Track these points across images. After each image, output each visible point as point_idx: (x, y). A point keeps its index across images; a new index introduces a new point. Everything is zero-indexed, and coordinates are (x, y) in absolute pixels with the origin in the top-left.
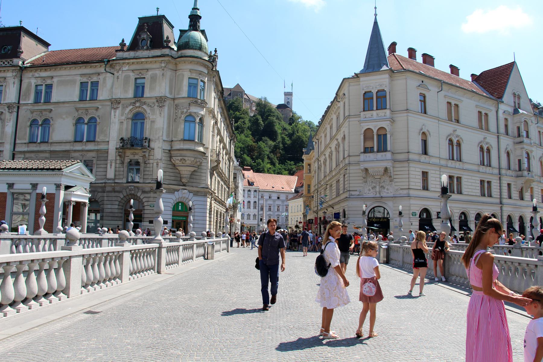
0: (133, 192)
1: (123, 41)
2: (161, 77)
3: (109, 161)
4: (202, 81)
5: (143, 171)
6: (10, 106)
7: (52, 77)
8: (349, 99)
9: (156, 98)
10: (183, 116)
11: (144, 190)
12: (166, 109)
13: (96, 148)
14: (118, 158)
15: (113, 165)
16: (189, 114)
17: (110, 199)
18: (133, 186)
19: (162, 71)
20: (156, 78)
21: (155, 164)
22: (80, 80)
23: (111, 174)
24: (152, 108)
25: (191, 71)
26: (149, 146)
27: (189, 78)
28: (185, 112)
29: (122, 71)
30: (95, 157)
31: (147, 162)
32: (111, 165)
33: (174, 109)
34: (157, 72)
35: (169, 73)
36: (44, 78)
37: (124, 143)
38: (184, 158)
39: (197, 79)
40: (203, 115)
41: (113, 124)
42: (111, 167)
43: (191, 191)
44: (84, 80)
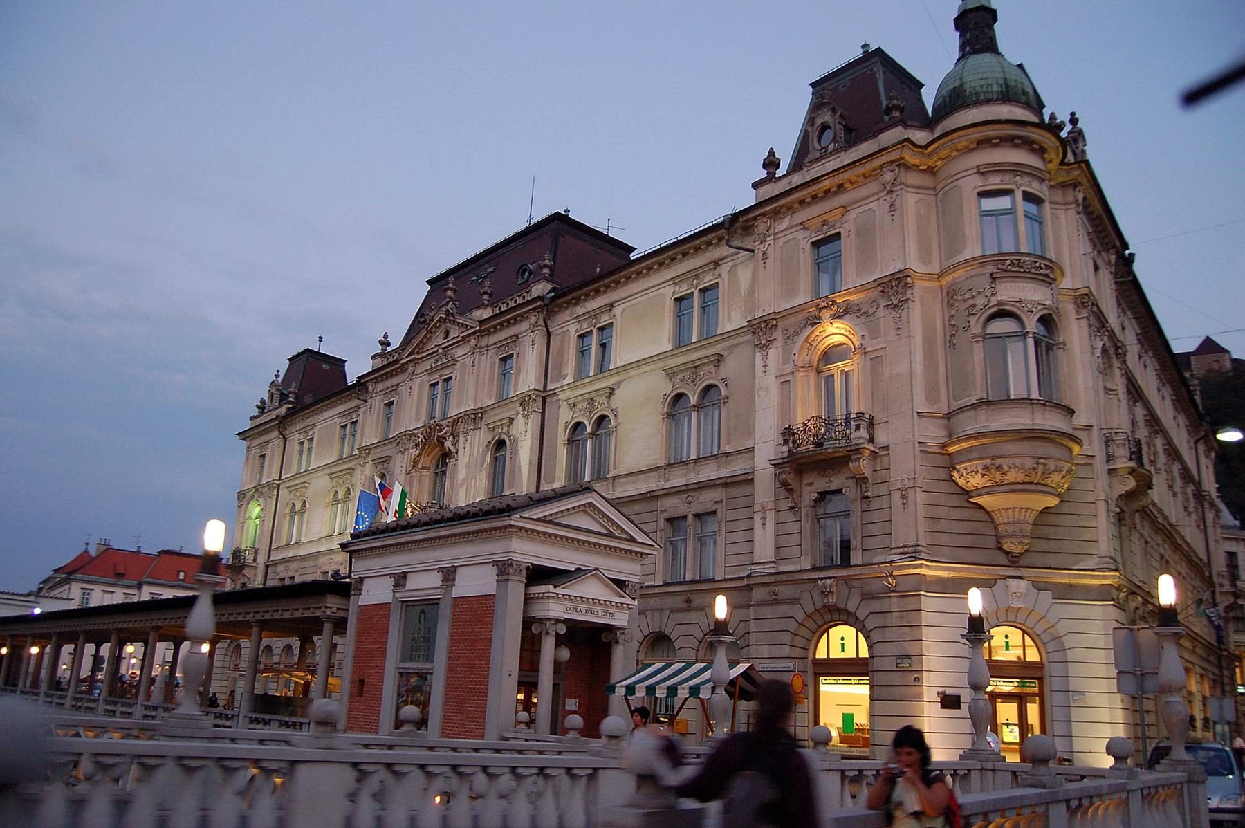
0: (831, 600)
1: (771, 153)
2: (887, 216)
3: (757, 508)
5: (859, 527)
6: (524, 402)
7: (611, 306)
9: (878, 283)
10: (973, 319)
11: (867, 588)
12: (914, 312)
13: (723, 473)
14: (782, 493)
15: (770, 516)
17: (766, 625)
18: (830, 578)
19: (888, 197)
20: (873, 224)
21: (896, 496)
22: (673, 294)
23: (764, 546)
24: (870, 319)
25: (982, 172)
26: (871, 440)
28: (979, 307)
29: (775, 234)
30: (721, 502)
31: (869, 494)
32: (764, 518)
33: (945, 307)
34: (872, 205)
35: (910, 201)
36: (594, 315)
37: (794, 442)
38: (998, 462)
41: (762, 394)
42: (764, 524)
43: (1042, 585)
44: (683, 290)
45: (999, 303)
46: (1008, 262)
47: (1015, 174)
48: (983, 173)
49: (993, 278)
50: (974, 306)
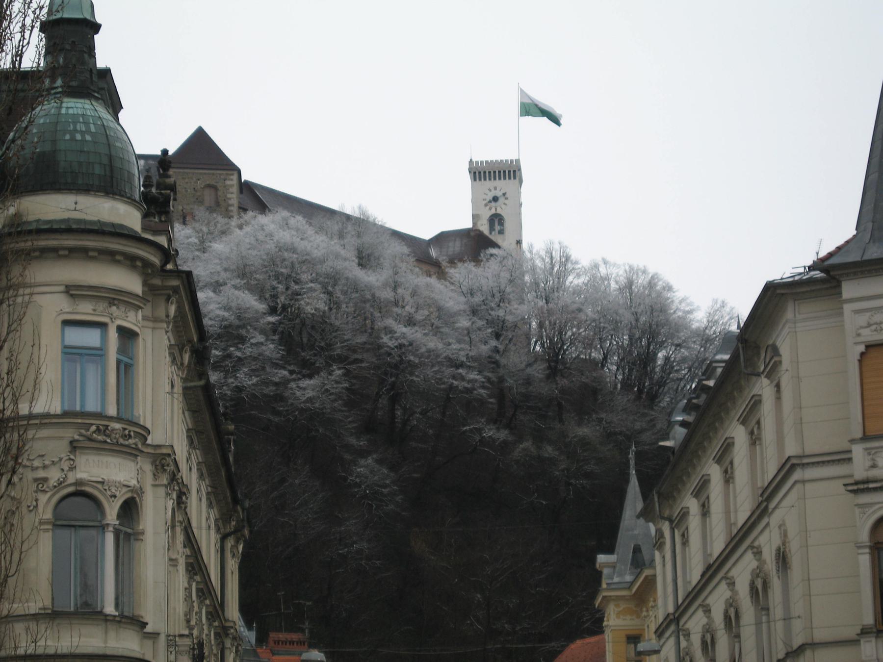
4: (121, 330)
8: (798, 378)
10: (43, 498)
16: (71, 489)
25: (73, 292)
27: (67, 323)
28: (52, 482)
39: (102, 326)
40: (133, 490)
45: (79, 483)
46: (94, 428)
47: (112, 302)
48: (72, 295)
49: (74, 447)
50: (45, 480)
